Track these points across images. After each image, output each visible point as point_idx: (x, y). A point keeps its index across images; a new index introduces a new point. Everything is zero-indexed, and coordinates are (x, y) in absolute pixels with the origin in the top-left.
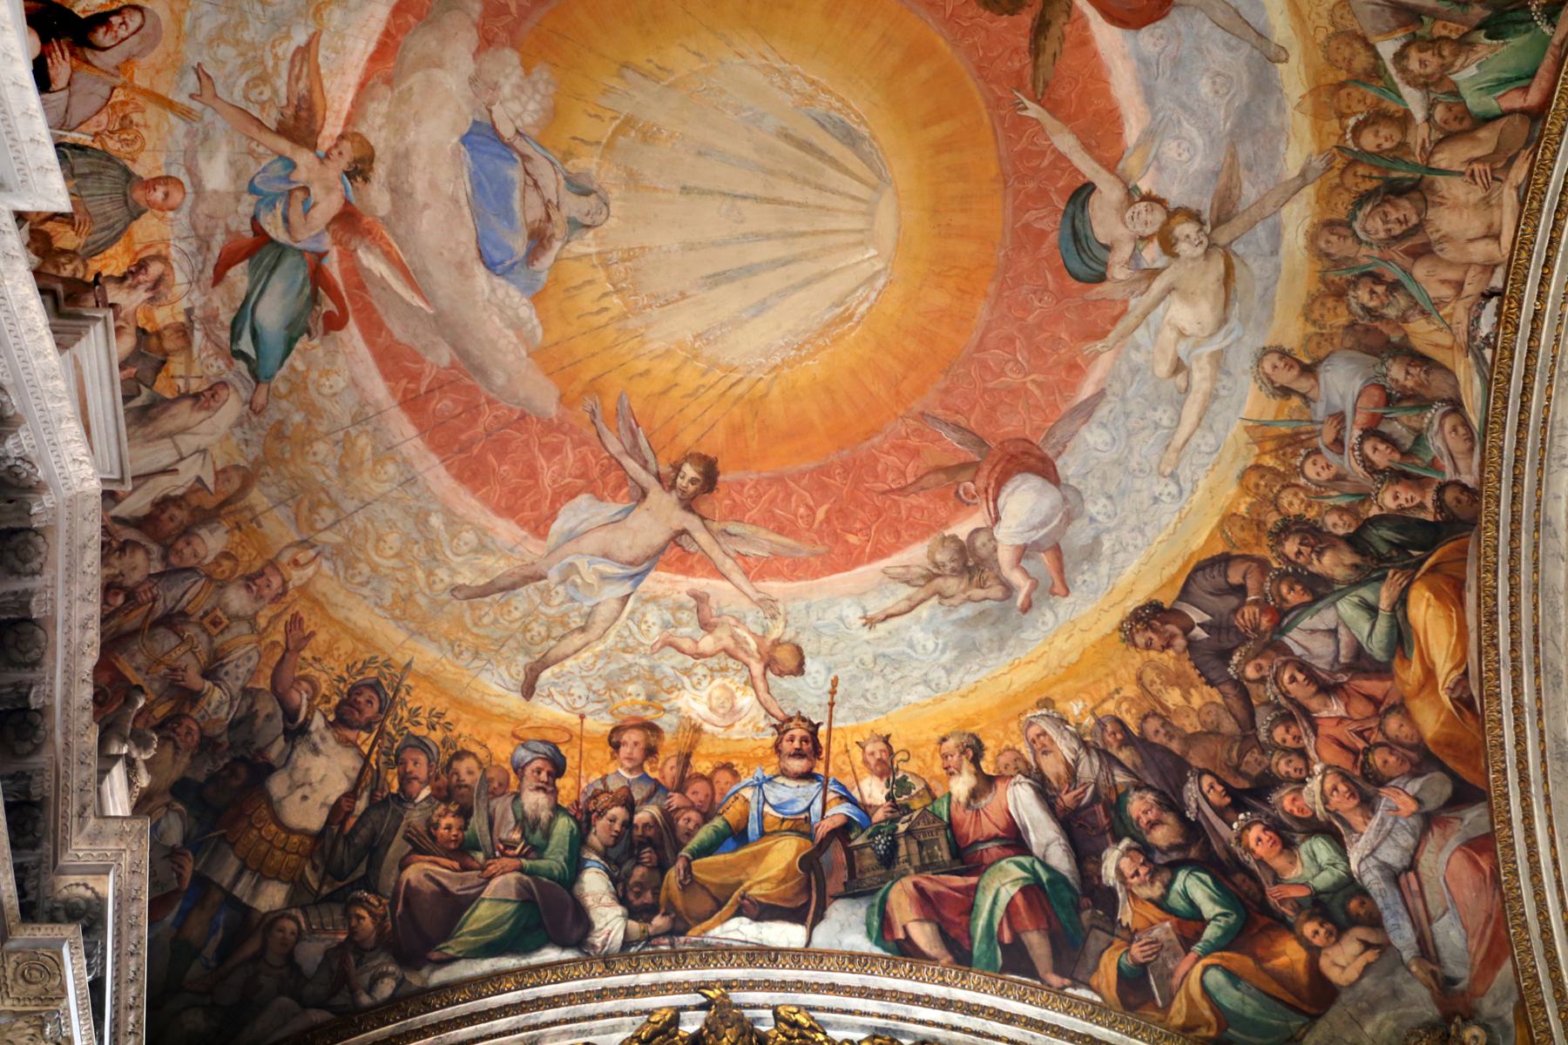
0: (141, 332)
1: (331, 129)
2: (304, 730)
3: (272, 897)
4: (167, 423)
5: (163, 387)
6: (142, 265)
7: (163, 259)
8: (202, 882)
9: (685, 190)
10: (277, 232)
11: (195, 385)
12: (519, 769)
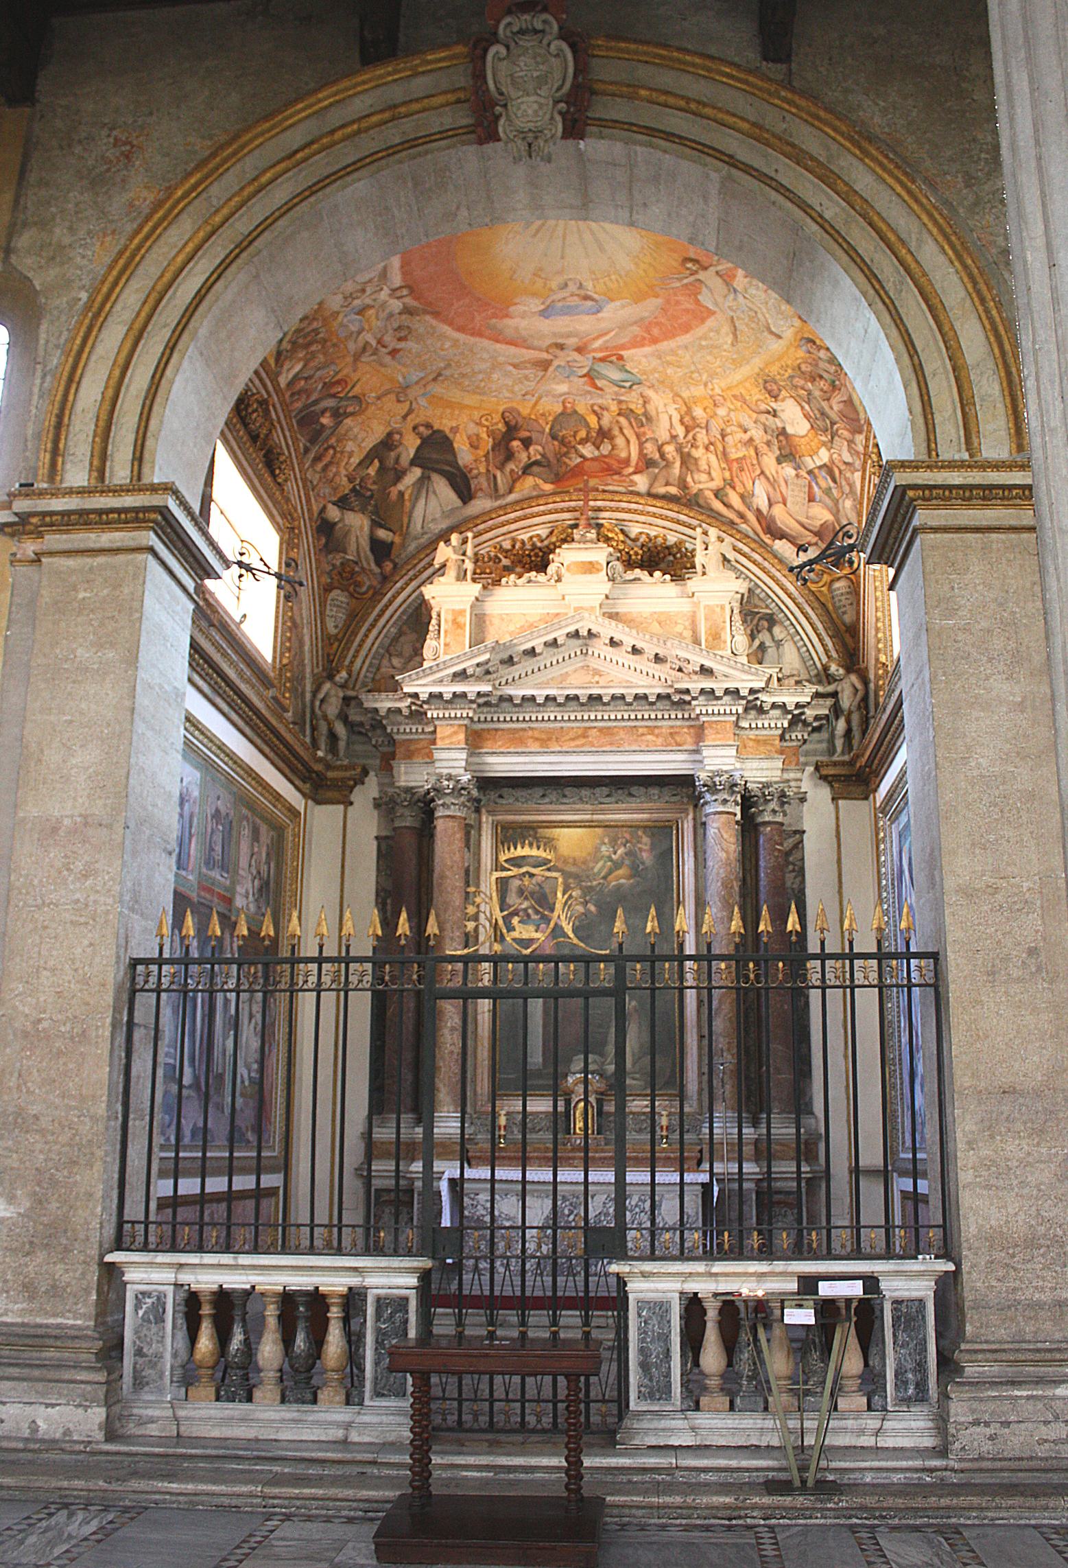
0: (619, 414)
1: (545, 356)
2: (775, 411)
3: (824, 456)
4: (653, 413)
5: (640, 411)
6: (595, 412)
7: (592, 406)
8: (810, 472)
9: (562, 258)
10: (585, 371)
11: (641, 401)
12: (809, 352)
